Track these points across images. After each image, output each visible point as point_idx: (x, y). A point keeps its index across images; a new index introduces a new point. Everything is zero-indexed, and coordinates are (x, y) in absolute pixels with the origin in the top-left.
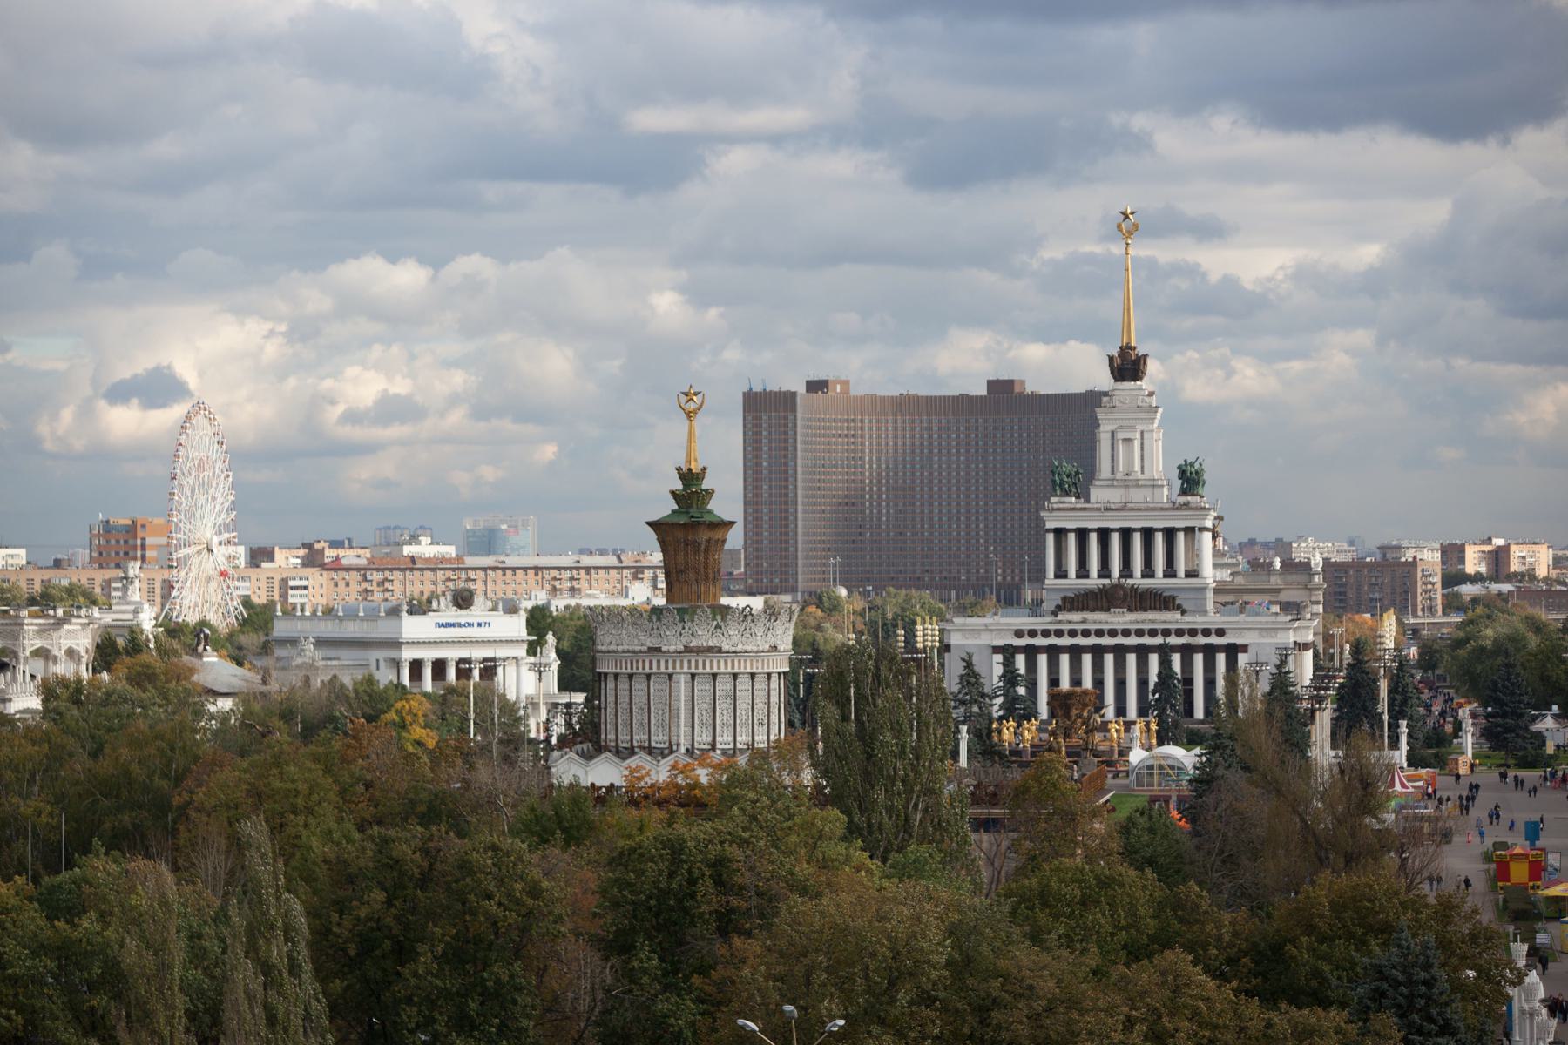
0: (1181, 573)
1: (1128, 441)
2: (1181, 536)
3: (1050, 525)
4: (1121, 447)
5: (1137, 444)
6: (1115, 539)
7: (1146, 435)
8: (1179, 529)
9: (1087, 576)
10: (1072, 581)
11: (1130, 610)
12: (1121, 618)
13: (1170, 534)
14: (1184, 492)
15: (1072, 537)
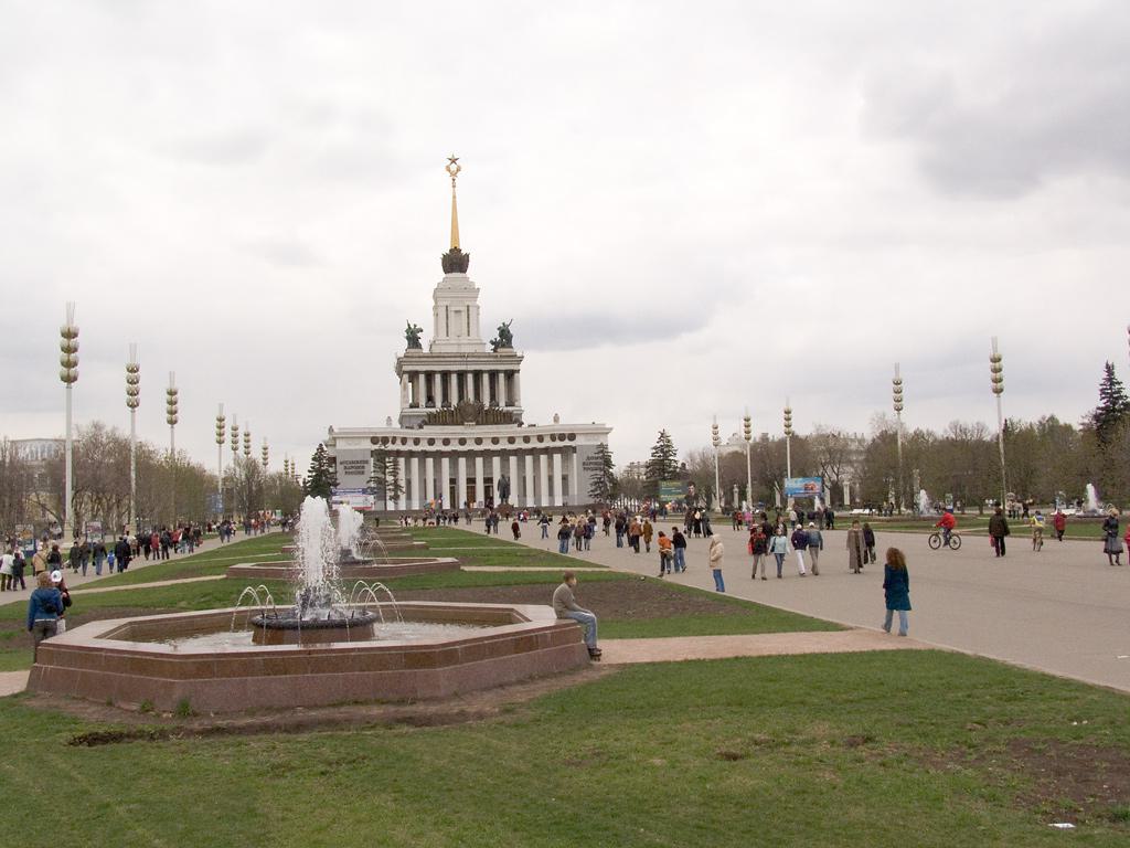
0: (502, 404)
1: (459, 311)
2: (502, 376)
3: (405, 368)
4: (452, 315)
5: (464, 315)
6: (454, 379)
7: (471, 309)
8: (498, 372)
9: (434, 407)
10: (423, 410)
11: (478, 424)
12: (471, 431)
13: (493, 375)
14: (503, 346)
15: (422, 378)
